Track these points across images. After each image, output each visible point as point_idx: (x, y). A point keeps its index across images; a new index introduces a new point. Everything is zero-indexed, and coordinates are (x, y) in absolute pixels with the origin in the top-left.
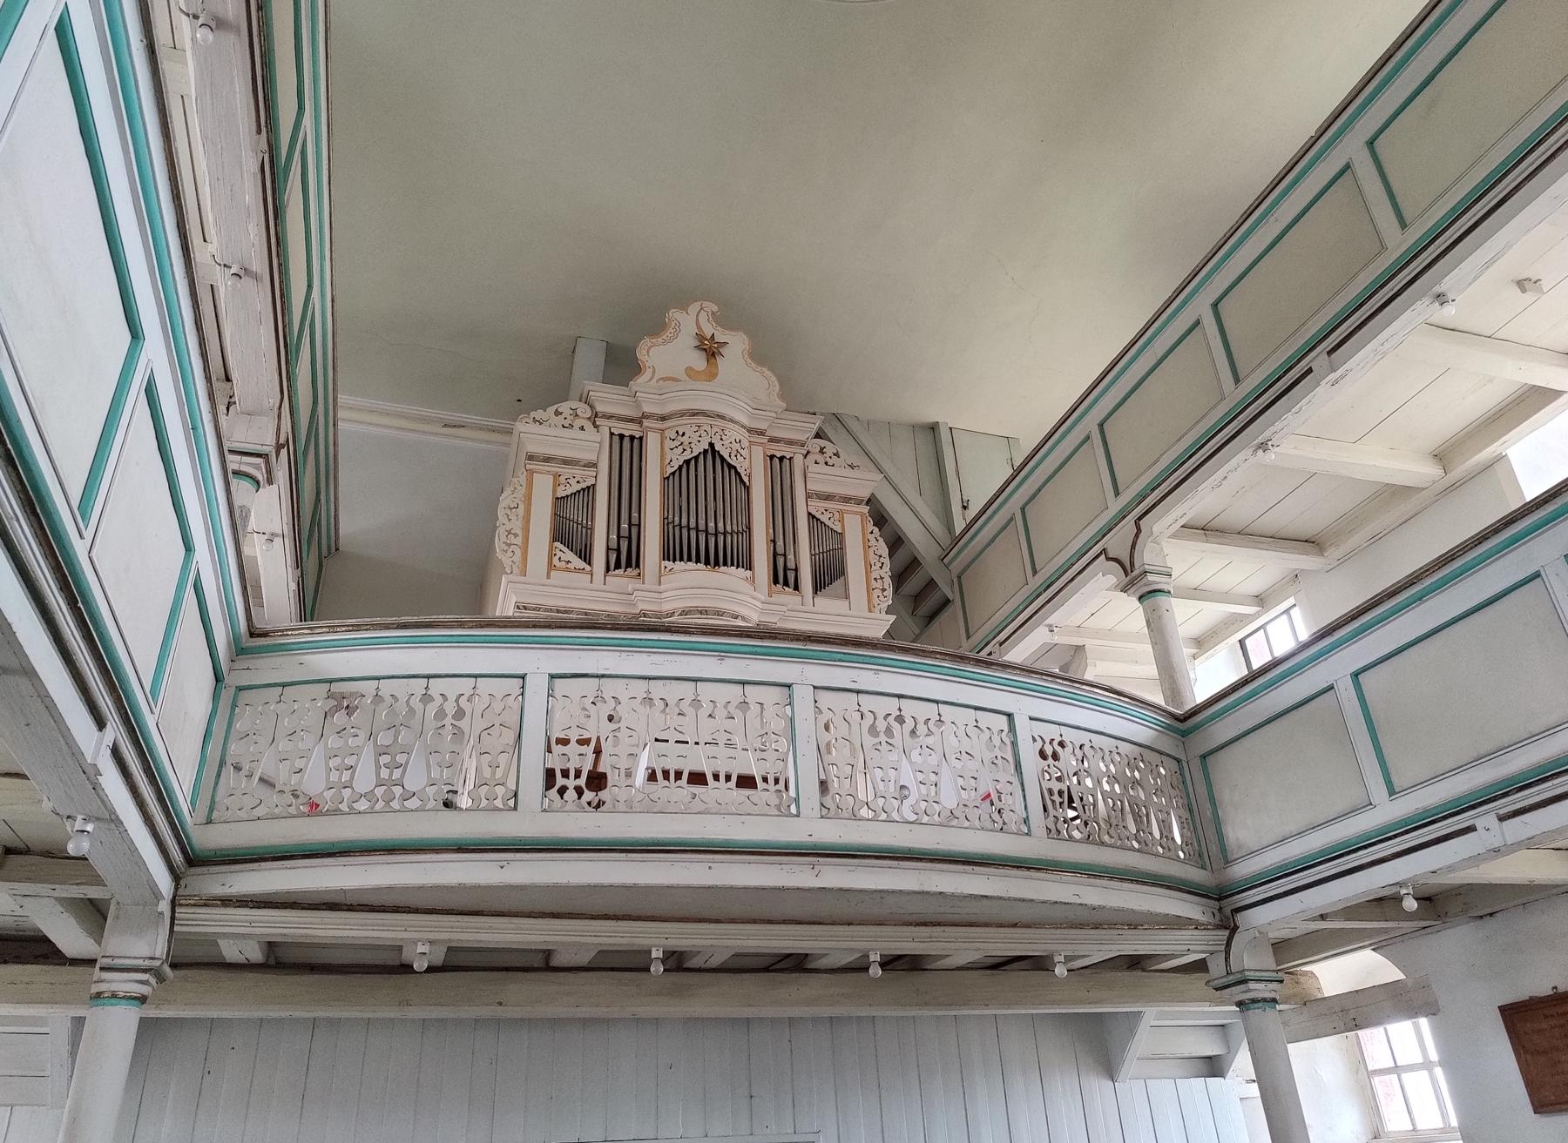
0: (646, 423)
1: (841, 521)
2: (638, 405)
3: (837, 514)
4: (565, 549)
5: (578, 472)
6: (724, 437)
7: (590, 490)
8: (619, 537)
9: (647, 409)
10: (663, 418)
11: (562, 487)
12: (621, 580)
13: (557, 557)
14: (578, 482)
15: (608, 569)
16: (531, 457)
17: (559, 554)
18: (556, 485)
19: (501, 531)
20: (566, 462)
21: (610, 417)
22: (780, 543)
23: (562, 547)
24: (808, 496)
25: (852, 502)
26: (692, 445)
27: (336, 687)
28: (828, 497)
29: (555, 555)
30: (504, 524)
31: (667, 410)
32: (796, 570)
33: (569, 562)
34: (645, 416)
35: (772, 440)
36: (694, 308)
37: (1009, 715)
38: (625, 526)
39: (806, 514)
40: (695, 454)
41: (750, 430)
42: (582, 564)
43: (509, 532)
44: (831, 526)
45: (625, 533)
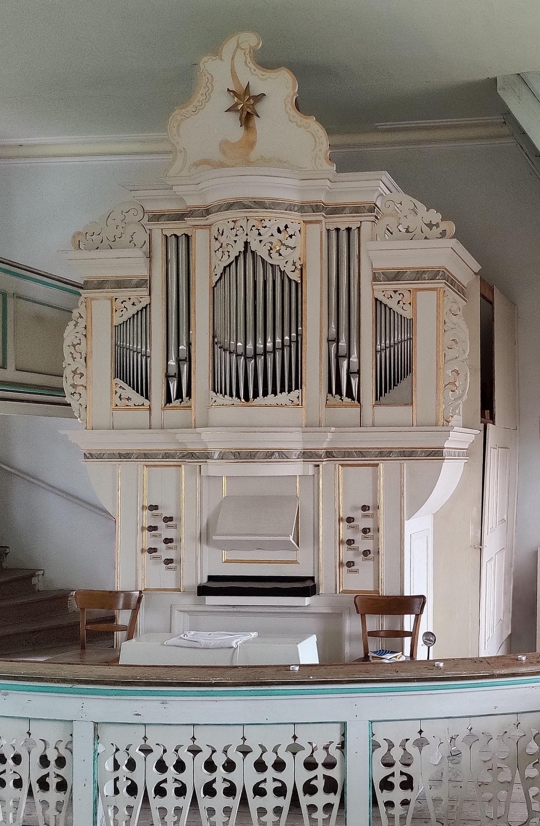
0: (190, 221)
2: (182, 200)
6: (262, 231)
9: (193, 202)
10: (207, 211)
11: (119, 313)
13: (118, 395)
14: (133, 304)
17: (120, 391)
18: (113, 311)
26: (230, 248)
29: (116, 392)
30: (69, 365)
31: (211, 199)
33: (129, 399)
34: (191, 213)
40: (232, 258)
42: (141, 400)
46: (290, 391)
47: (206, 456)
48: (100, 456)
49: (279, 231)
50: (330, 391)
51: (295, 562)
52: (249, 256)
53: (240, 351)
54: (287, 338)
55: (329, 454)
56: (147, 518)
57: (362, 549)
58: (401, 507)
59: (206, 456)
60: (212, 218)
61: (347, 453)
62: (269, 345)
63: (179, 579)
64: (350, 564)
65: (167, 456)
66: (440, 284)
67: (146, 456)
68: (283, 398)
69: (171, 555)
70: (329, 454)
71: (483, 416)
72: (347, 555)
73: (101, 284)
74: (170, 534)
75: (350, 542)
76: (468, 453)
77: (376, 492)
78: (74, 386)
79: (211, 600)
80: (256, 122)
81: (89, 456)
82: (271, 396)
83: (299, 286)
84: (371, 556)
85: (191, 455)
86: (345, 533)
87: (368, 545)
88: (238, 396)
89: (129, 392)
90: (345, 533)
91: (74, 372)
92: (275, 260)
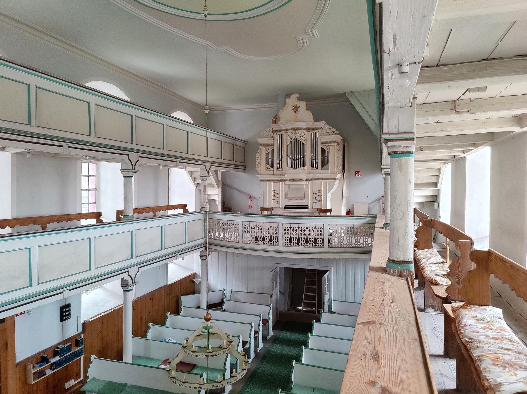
1: (329, 148)
3: (328, 146)
4: (268, 166)
5: (270, 147)
7: (273, 150)
8: (279, 160)
10: (287, 130)
12: (279, 172)
15: (277, 169)
16: (261, 145)
17: (267, 167)
19: (257, 163)
20: (268, 145)
21: (276, 131)
22: (314, 157)
23: (268, 165)
24: (321, 143)
25: (332, 142)
26: (292, 138)
27: (218, 220)
28: (326, 142)
31: (287, 128)
32: (318, 163)
33: (269, 168)
35: (313, 129)
36: (292, 97)
37: (324, 224)
38: (280, 158)
39: (321, 148)
40: (292, 140)
41: (306, 129)
43: (258, 163)
44: (327, 150)
45: (280, 159)
46: (303, 167)
47: (286, 180)
48: (264, 180)
49: (302, 134)
50: (311, 167)
51: (304, 202)
52: (296, 139)
53: (294, 159)
54: (303, 156)
55: (311, 180)
56: (273, 193)
57: (318, 199)
58: (327, 191)
59: (286, 180)
60: (287, 131)
61: (315, 180)
62: (298, 158)
63: (279, 206)
64: (316, 202)
65: (277, 180)
66: (336, 144)
67: (273, 180)
68: (302, 168)
69: (278, 200)
70: (311, 180)
71: (343, 171)
72: (315, 201)
73: (264, 145)
74: (278, 196)
75: (316, 198)
76: (339, 180)
77: (321, 187)
78: (258, 166)
79: (287, 209)
80: (297, 112)
81: (261, 180)
82: (300, 168)
83: (306, 145)
84: (320, 201)
85: (283, 180)
86: (315, 196)
87: (319, 199)
88: (293, 168)
89: (269, 167)
90: (315, 196)
91: (258, 163)
92: (301, 140)
